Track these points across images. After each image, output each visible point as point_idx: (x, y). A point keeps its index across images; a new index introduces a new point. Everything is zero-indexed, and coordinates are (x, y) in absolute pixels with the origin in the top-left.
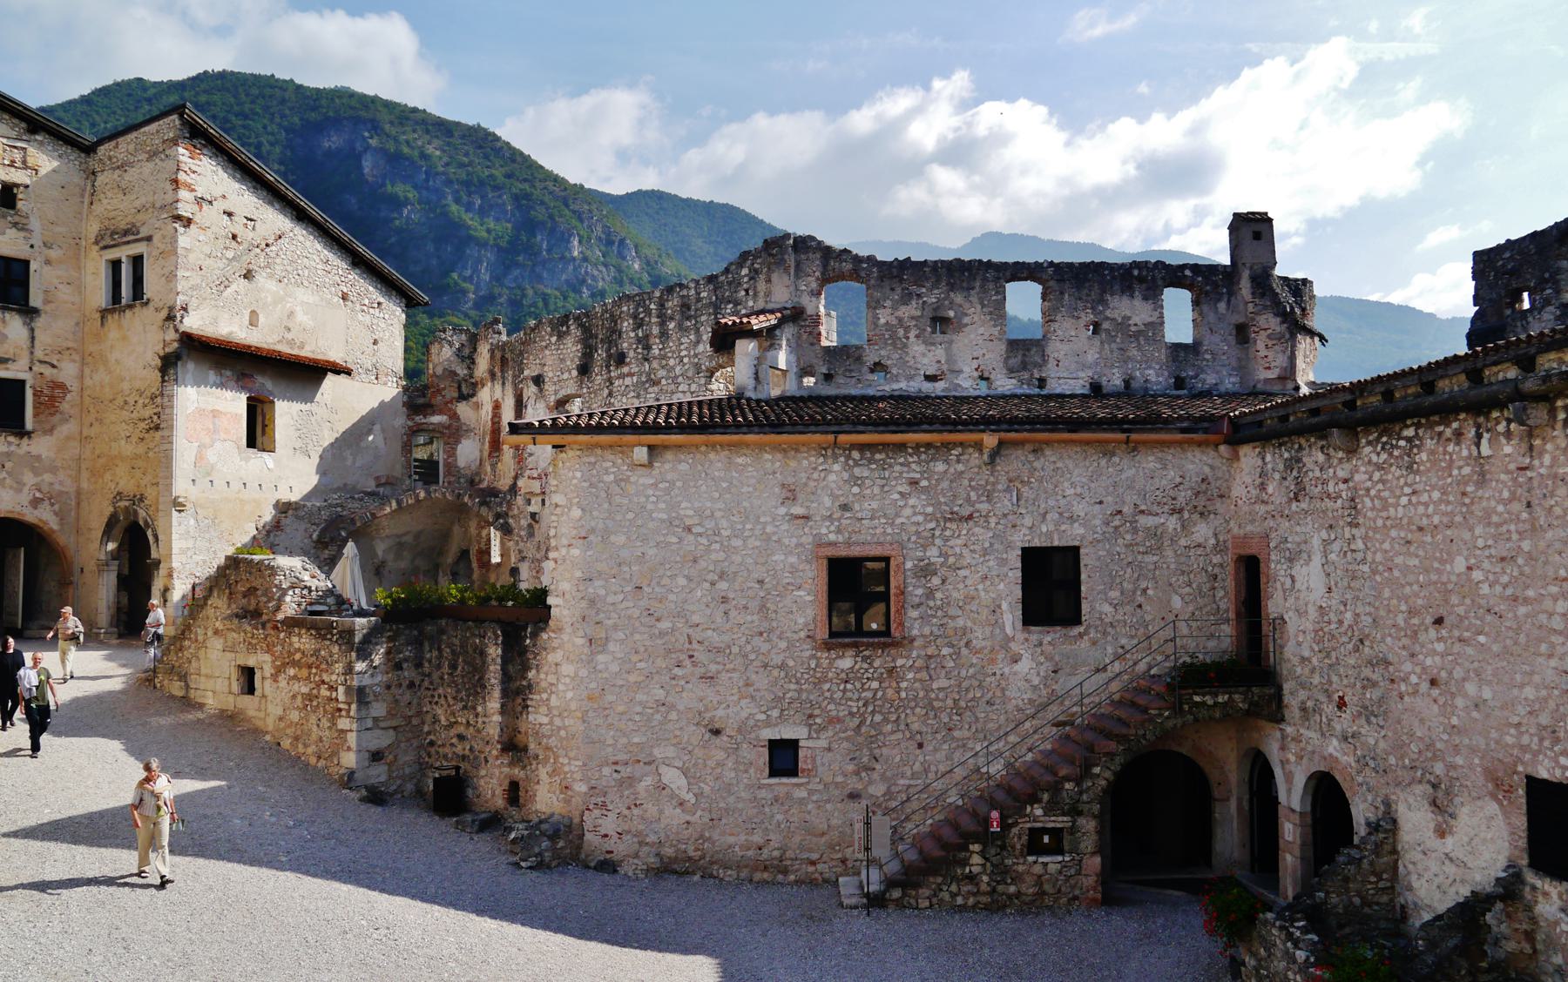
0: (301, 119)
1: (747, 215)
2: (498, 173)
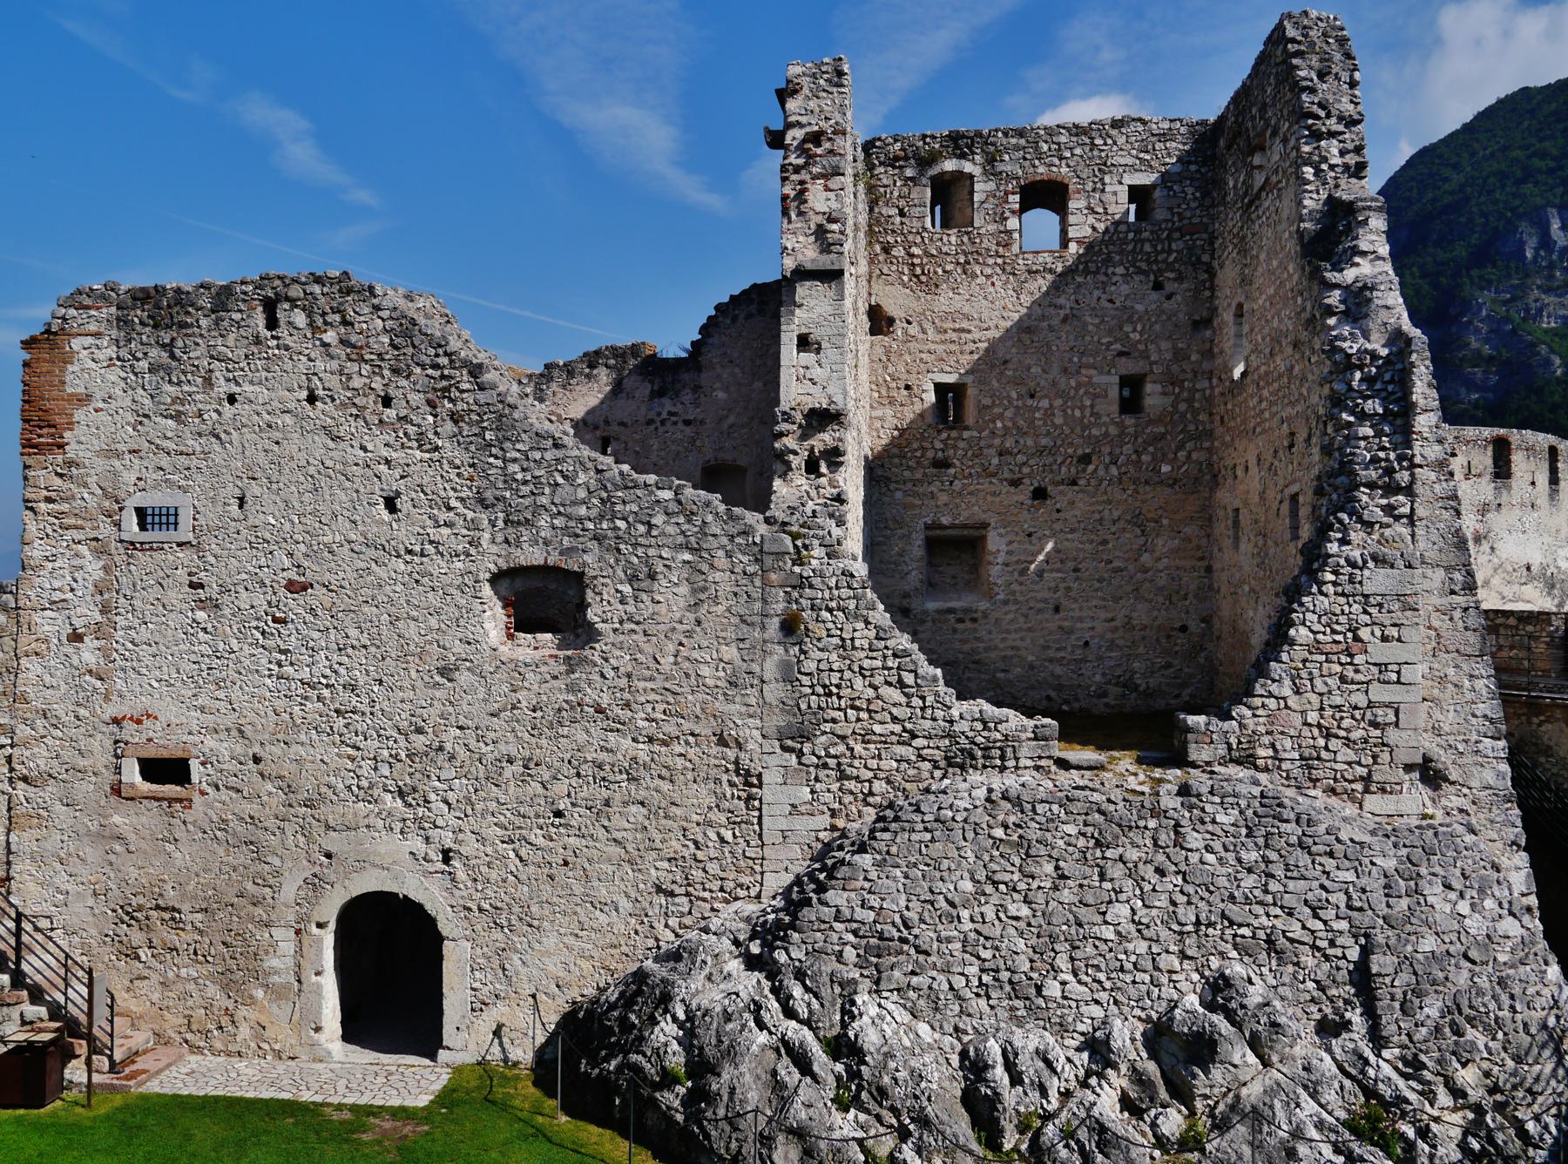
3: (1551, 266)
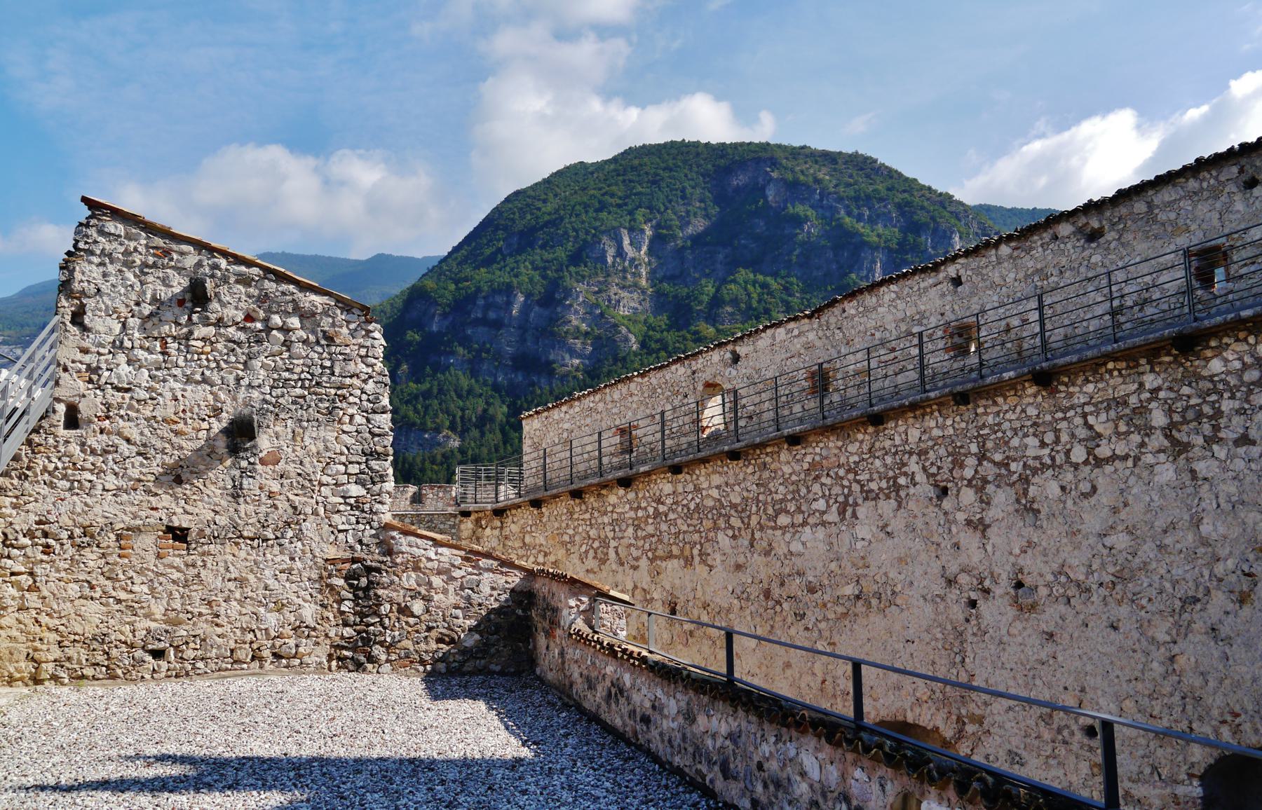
0: (713, 166)
3: (624, 270)
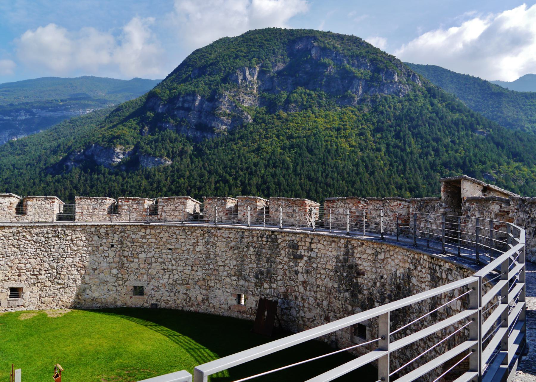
1: (443, 69)
2: (363, 51)
3: (246, 86)
